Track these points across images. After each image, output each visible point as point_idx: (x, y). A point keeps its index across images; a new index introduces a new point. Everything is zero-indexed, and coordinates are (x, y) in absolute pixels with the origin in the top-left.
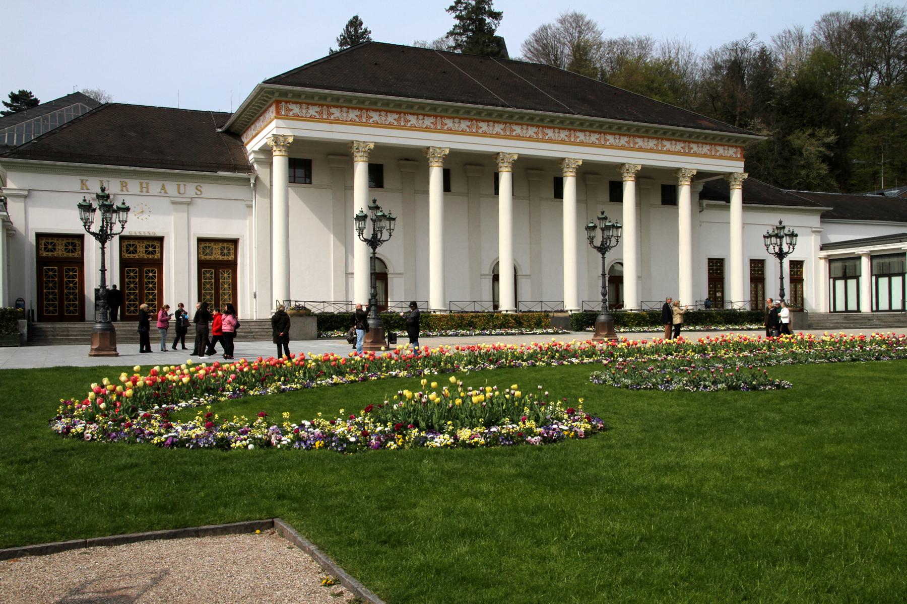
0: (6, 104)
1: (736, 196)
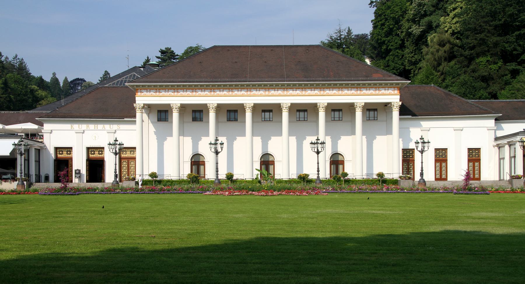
0: (157, 57)
1: (396, 113)
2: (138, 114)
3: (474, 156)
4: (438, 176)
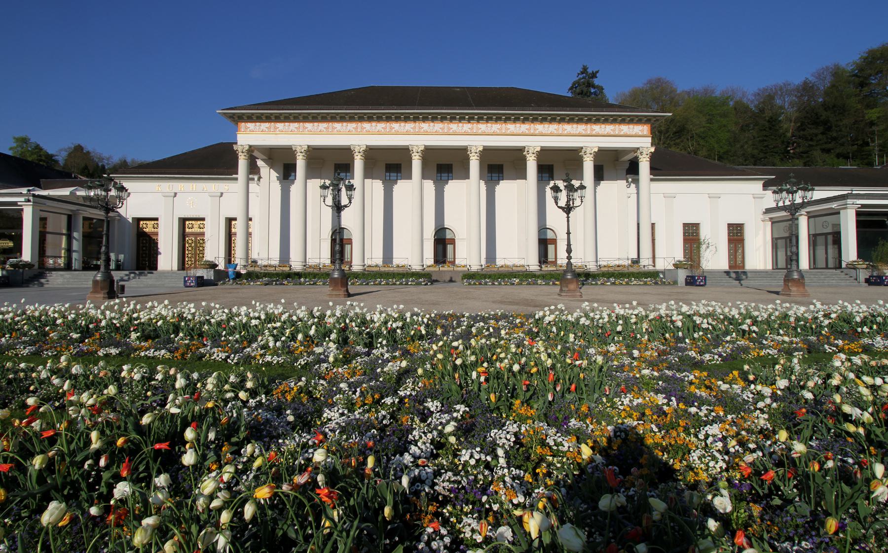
1: (644, 167)
2: (242, 164)
3: (736, 234)
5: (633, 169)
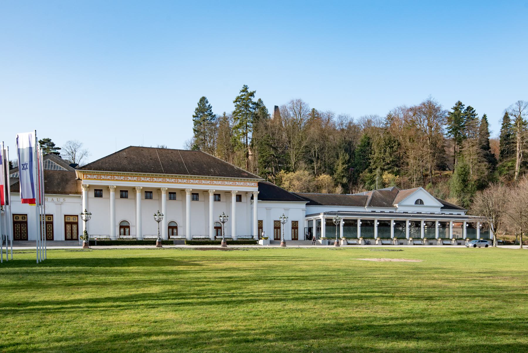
1: (256, 198)
4: (276, 237)
5: (252, 198)
